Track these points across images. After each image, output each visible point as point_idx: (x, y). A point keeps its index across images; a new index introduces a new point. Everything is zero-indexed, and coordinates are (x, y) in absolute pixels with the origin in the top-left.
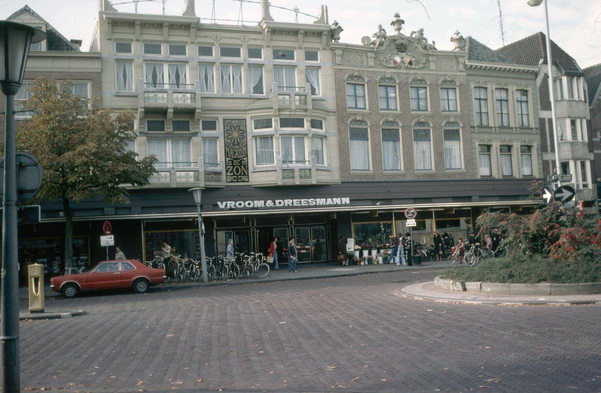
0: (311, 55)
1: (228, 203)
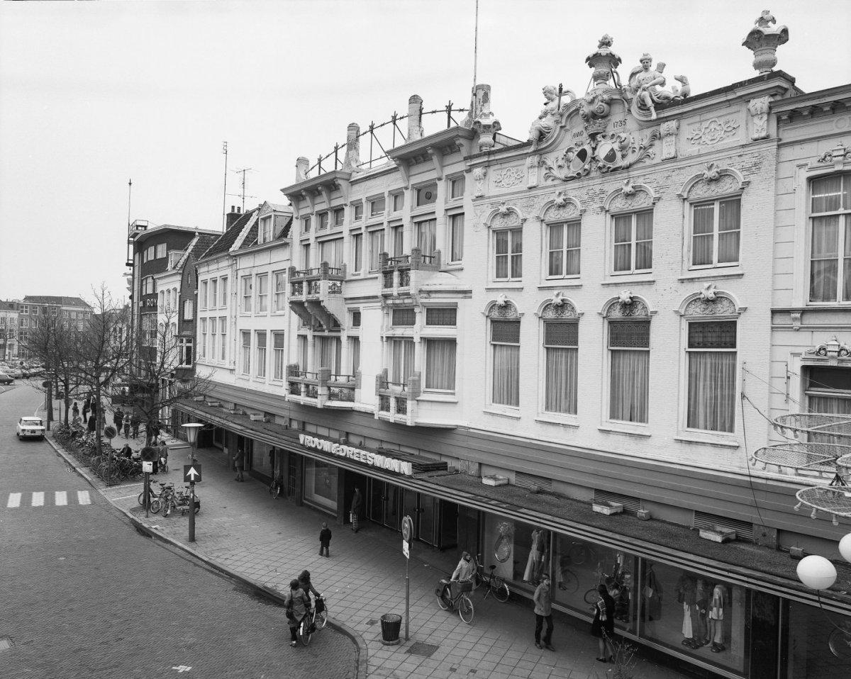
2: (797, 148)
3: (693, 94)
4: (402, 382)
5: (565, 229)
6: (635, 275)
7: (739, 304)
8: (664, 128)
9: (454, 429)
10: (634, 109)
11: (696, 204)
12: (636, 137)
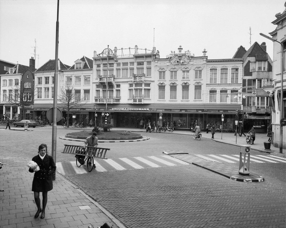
0: (149, 63)
2: (209, 65)
3: (195, 56)
7: (202, 83)
8: (191, 60)
9: (150, 104)
10: (187, 57)
11: (160, 72)
12: (187, 61)
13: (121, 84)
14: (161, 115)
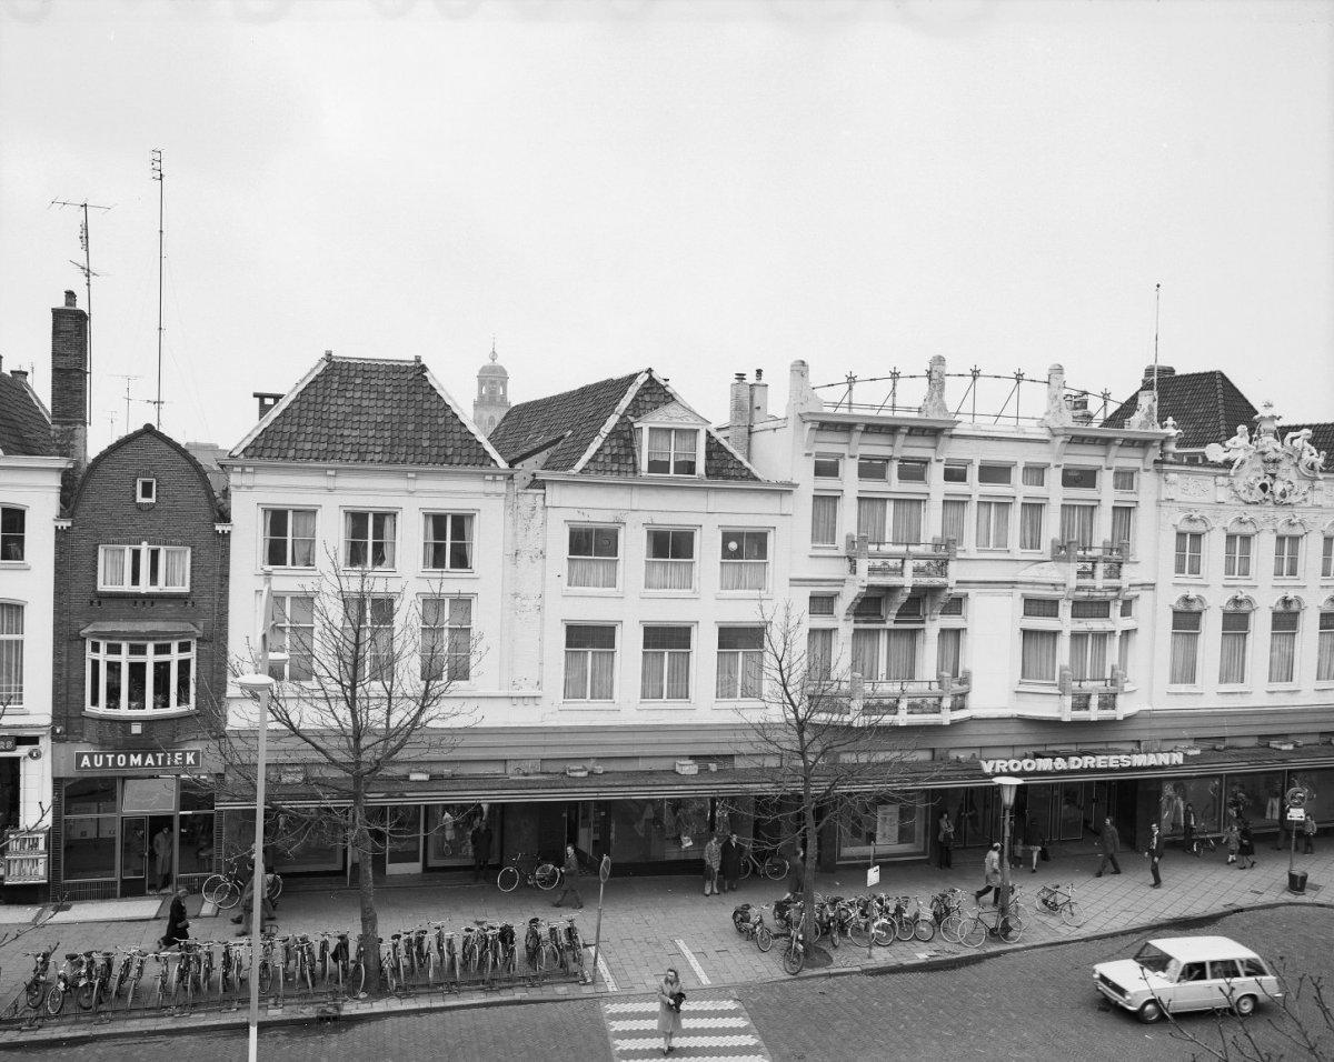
0: (1125, 479)
1: (999, 762)
4: (1108, 676)
5: (1238, 543)
6: (1288, 581)
13: (972, 592)
14: (1302, 799)
